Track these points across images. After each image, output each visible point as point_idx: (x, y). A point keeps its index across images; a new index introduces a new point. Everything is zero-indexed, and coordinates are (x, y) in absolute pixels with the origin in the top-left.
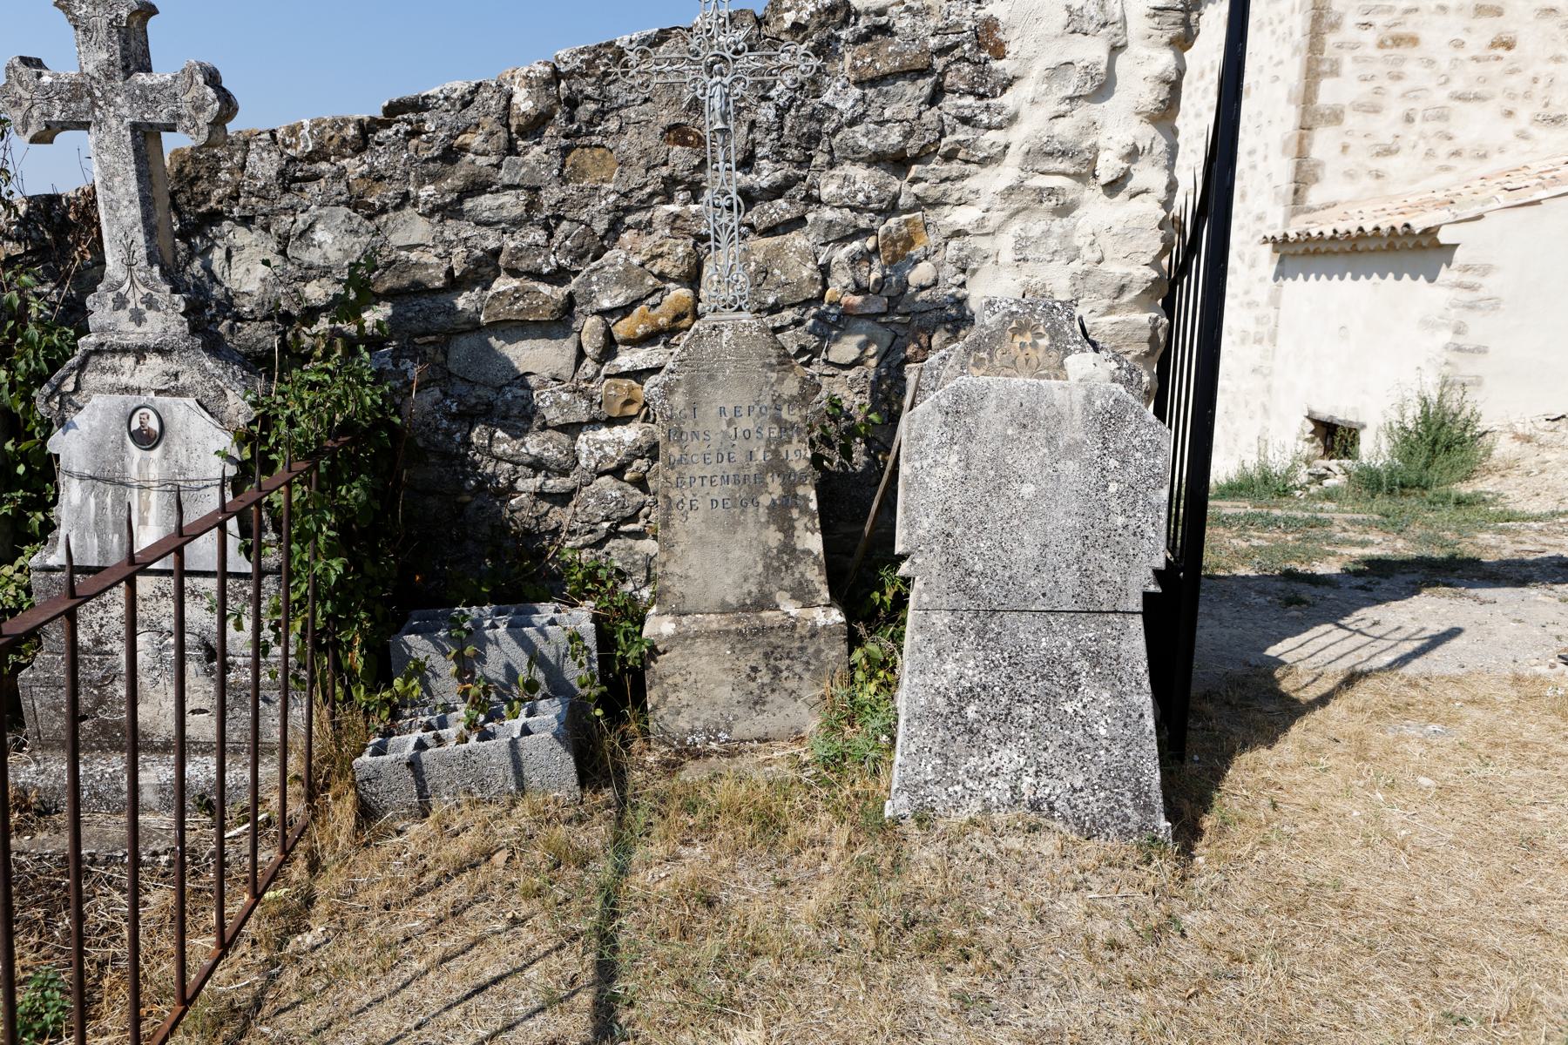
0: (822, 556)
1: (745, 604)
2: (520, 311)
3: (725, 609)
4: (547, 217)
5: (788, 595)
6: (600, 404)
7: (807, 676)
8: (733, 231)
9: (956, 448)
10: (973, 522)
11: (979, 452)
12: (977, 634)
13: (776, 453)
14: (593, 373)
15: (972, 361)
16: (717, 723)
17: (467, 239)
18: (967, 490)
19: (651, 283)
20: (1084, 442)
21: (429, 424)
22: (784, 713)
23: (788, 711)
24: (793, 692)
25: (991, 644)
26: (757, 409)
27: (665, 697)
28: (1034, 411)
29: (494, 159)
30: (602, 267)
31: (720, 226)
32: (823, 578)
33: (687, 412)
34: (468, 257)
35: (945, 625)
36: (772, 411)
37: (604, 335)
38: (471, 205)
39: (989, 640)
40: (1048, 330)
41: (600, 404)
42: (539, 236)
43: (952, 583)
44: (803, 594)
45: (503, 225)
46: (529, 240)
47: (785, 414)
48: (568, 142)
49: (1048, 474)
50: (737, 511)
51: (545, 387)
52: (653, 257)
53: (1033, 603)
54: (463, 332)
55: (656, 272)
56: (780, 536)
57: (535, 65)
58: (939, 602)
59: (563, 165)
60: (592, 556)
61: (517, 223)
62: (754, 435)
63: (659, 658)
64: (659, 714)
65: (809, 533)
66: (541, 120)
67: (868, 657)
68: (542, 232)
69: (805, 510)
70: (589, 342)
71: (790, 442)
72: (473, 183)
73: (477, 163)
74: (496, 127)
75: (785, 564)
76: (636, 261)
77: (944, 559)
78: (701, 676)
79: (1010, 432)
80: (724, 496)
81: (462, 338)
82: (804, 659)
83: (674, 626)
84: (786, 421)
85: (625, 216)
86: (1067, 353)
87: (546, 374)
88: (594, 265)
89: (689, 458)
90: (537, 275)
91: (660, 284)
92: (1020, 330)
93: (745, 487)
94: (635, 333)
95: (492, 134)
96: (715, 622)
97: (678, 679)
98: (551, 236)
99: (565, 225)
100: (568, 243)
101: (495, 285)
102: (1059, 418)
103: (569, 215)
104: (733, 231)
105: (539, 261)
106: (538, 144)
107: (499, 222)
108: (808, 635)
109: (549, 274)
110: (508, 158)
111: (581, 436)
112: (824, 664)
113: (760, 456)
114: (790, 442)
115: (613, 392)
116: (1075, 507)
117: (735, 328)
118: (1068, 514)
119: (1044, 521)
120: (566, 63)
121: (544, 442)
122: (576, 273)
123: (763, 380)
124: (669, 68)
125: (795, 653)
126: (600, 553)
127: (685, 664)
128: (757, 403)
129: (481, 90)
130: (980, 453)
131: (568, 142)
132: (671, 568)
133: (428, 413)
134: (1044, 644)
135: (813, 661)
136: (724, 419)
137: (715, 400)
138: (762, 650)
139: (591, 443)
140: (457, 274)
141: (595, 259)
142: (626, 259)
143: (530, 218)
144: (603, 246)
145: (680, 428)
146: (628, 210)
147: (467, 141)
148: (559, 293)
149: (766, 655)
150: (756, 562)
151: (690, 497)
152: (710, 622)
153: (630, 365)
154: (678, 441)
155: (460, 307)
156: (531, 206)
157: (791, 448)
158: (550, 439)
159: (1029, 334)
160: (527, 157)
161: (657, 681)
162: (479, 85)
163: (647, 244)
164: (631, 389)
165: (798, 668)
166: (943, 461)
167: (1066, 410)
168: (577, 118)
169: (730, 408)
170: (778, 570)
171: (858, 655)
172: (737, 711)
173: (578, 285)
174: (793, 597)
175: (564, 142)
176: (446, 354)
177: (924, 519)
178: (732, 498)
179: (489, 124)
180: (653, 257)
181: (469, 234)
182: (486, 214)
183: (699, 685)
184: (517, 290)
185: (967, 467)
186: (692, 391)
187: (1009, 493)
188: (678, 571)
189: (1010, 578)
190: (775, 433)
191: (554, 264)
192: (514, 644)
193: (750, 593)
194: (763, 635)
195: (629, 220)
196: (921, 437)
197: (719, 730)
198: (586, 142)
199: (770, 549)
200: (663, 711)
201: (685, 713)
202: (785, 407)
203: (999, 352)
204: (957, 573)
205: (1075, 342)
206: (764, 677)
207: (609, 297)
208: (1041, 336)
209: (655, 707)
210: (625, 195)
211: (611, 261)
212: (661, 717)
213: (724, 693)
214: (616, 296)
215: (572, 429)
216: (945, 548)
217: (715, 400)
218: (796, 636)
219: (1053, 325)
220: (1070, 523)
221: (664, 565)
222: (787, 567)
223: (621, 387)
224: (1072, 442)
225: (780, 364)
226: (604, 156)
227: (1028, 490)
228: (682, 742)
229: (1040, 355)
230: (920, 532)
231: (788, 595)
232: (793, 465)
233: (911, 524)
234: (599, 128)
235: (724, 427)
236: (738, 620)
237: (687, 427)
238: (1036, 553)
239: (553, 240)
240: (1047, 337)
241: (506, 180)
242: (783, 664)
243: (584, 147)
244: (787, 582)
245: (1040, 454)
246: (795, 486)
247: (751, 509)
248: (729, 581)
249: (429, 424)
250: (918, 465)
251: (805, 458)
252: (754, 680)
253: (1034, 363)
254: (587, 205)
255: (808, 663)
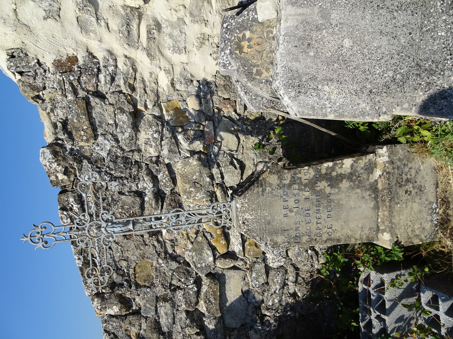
0: (354, 159)
1: (375, 197)
2: (215, 299)
3: (377, 208)
4: (171, 291)
5: (371, 175)
6: (257, 258)
7: (410, 165)
8: (189, 214)
9: (320, 87)
10: (364, 77)
11: (324, 72)
12: (432, 75)
13: (306, 185)
14: (242, 262)
15: (258, 77)
16: (429, 209)
17: (182, 328)
18: (345, 80)
19: (201, 238)
20: (320, 7)
21: (266, 335)
22: (425, 176)
23: (425, 174)
24: (416, 172)
25: (440, 66)
26: (284, 197)
27: (417, 236)
28: (300, 39)
29: (143, 321)
30: (194, 262)
31: (187, 221)
32: (364, 158)
33: (286, 234)
34: (190, 327)
35: (424, 94)
36: (286, 188)
37: (225, 259)
38: (165, 328)
39: (437, 67)
40: (241, 32)
41: (257, 258)
42: (179, 294)
43: (398, 90)
44: (371, 168)
45: (175, 311)
46: (181, 298)
47: (287, 182)
48: (133, 285)
49: (339, 30)
50: (333, 204)
51: (248, 283)
52: (188, 238)
53: (414, 40)
54: (224, 323)
55: (195, 236)
56: (344, 181)
57: (94, 306)
58: (409, 98)
59: (145, 286)
60: (322, 256)
61: (174, 305)
62: (297, 198)
63: (400, 240)
64: (424, 238)
65: (343, 166)
66: (122, 300)
67: (404, 134)
68: (177, 292)
69: (333, 169)
70: (229, 265)
71: (301, 178)
72: (155, 329)
73: (145, 328)
74: (127, 321)
75: (357, 178)
76: (190, 246)
77: (384, 94)
78: (409, 219)
79: (312, 54)
80: (326, 211)
81: (226, 322)
82: (402, 167)
83: (385, 234)
84: (290, 181)
85: (169, 253)
86: (255, 20)
87: (242, 283)
88: (192, 266)
89: (308, 231)
90: (198, 293)
91: (201, 234)
92: (240, 48)
93: (322, 201)
94: (225, 244)
95: (130, 323)
96: (383, 213)
97: (410, 230)
98: (179, 288)
99: (174, 282)
100: (182, 280)
101: (203, 312)
102: (305, 23)
103: (169, 281)
104: (189, 214)
105: (191, 293)
106: (134, 299)
107: (173, 314)
108: (392, 165)
109: (197, 287)
110: (142, 314)
111: (270, 265)
112: (405, 156)
113: (307, 194)
114: (301, 178)
115: (252, 253)
116: (359, 13)
117: (244, 212)
118: (363, 18)
119: (366, 33)
120: (92, 291)
121: (274, 283)
122: (197, 274)
123: (270, 195)
124: (98, 258)
125: (400, 172)
126: (320, 253)
127: (403, 227)
128: (281, 197)
129: (108, 330)
130: (324, 72)
131: (133, 285)
132: (358, 236)
133: (261, 335)
134: (443, 34)
135: (404, 162)
136: (290, 214)
137: (280, 220)
138: (398, 189)
139: (274, 261)
140: (199, 331)
141: (190, 266)
142: (190, 251)
143: (171, 299)
144: (183, 263)
145: (294, 238)
146: (166, 252)
147: (134, 334)
148: (206, 281)
149: (400, 186)
150: (356, 193)
151: (326, 229)
152: (384, 215)
153: (239, 246)
154: (300, 237)
155: (214, 327)
156: (165, 299)
157: (304, 177)
158: (273, 280)
159: (243, 43)
160: (141, 304)
161: (410, 240)
162: (106, 331)
163: (182, 242)
164: (250, 245)
165: (406, 169)
166: (327, 95)
167: (300, 18)
168: (121, 282)
169: (284, 212)
170: (360, 181)
171: (402, 139)
172: (424, 199)
173: (202, 273)
174: (372, 173)
175: (133, 288)
176: (233, 329)
177: (361, 106)
178: (327, 207)
179: (125, 325)
180: (188, 238)
181: (179, 327)
182: (170, 320)
183: (412, 219)
184: (205, 302)
185: (331, 80)
186: (275, 232)
187: (348, 55)
188: (359, 232)
189: (398, 55)
190: (296, 186)
191: (193, 285)
192: (393, 312)
193: (370, 195)
194: (392, 188)
195: (170, 251)
196: (313, 108)
197: (432, 208)
198: (133, 276)
199: (350, 186)
200: (423, 236)
201: (424, 225)
202: (284, 182)
203: (253, 61)
204: (393, 87)
205: (248, 15)
206: (410, 187)
207: (208, 258)
208: (244, 35)
209: (421, 240)
210: (159, 255)
211: (191, 258)
212: (426, 237)
213: (416, 206)
214: (207, 255)
215: (268, 269)
216: (378, 94)
217: (280, 220)
218: (392, 171)
219: (238, 28)
220: (368, 17)
221: (356, 240)
222: (359, 177)
223: (249, 249)
224: (320, 15)
225: (262, 186)
226: (139, 267)
227: (347, 43)
228: (436, 226)
229: (255, 36)
230: (368, 108)
231: (371, 175)
232: (311, 176)
233: (363, 114)
234: (125, 270)
235: (294, 214)
236: (384, 201)
237: (293, 233)
238: (385, 38)
239: (181, 287)
240: (245, 32)
241: (153, 313)
242: (404, 177)
243: (135, 277)
244: (365, 176)
245: (326, 35)
246: (321, 174)
247: (332, 197)
248: (364, 206)
249: (266, 335)
250: (329, 110)
251: (308, 170)
252: (411, 192)
253: (260, 40)
254: (164, 273)
255: (404, 165)
